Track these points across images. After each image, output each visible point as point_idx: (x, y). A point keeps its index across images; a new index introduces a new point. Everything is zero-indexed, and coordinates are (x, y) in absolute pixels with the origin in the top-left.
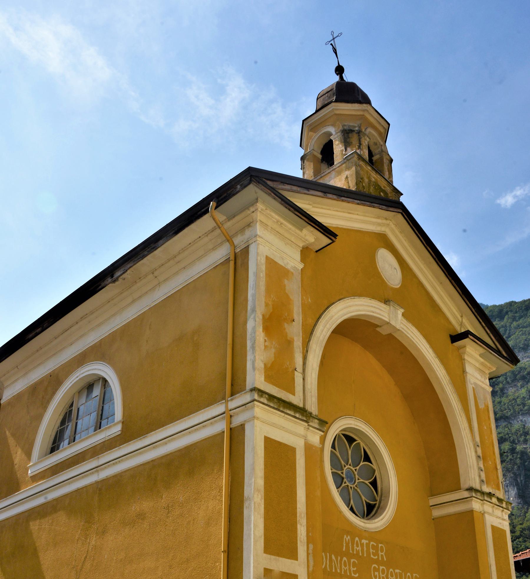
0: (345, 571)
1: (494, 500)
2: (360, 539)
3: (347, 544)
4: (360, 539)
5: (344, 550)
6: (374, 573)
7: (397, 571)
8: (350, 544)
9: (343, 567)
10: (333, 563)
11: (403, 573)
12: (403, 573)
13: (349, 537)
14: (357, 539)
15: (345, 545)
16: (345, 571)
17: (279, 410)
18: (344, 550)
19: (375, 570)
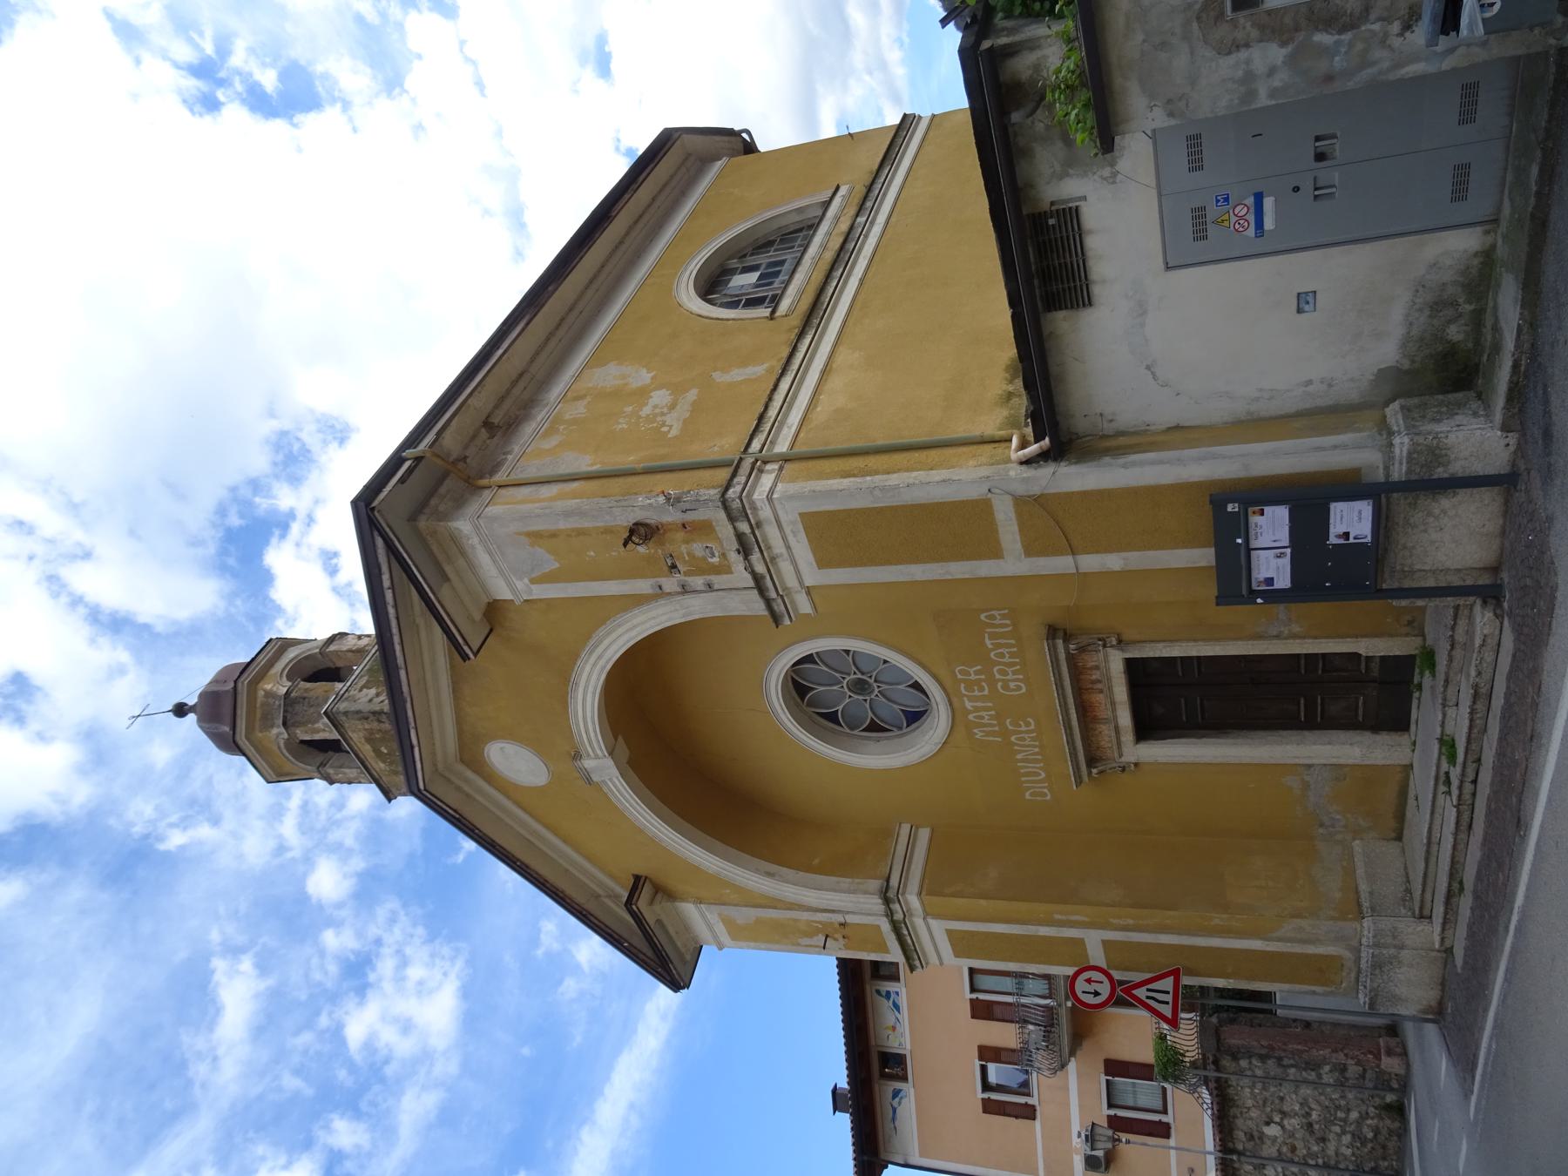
0: (1033, 739)
1: (755, 557)
2: (970, 712)
3: (988, 734)
4: (970, 712)
5: (999, 739)
6: (1013, 690)
7: (988, 642)
8: (985, 729)
9: (1027, 743)
10: (1029, 757)
11: (988, 630)
12: (988, 630)
13: (975, 731)
14: (971, 717)
15: (991, 739)
16: (1033, 739)
17: (916, 950)
18: (999, 739)
19: (1006, 687)
